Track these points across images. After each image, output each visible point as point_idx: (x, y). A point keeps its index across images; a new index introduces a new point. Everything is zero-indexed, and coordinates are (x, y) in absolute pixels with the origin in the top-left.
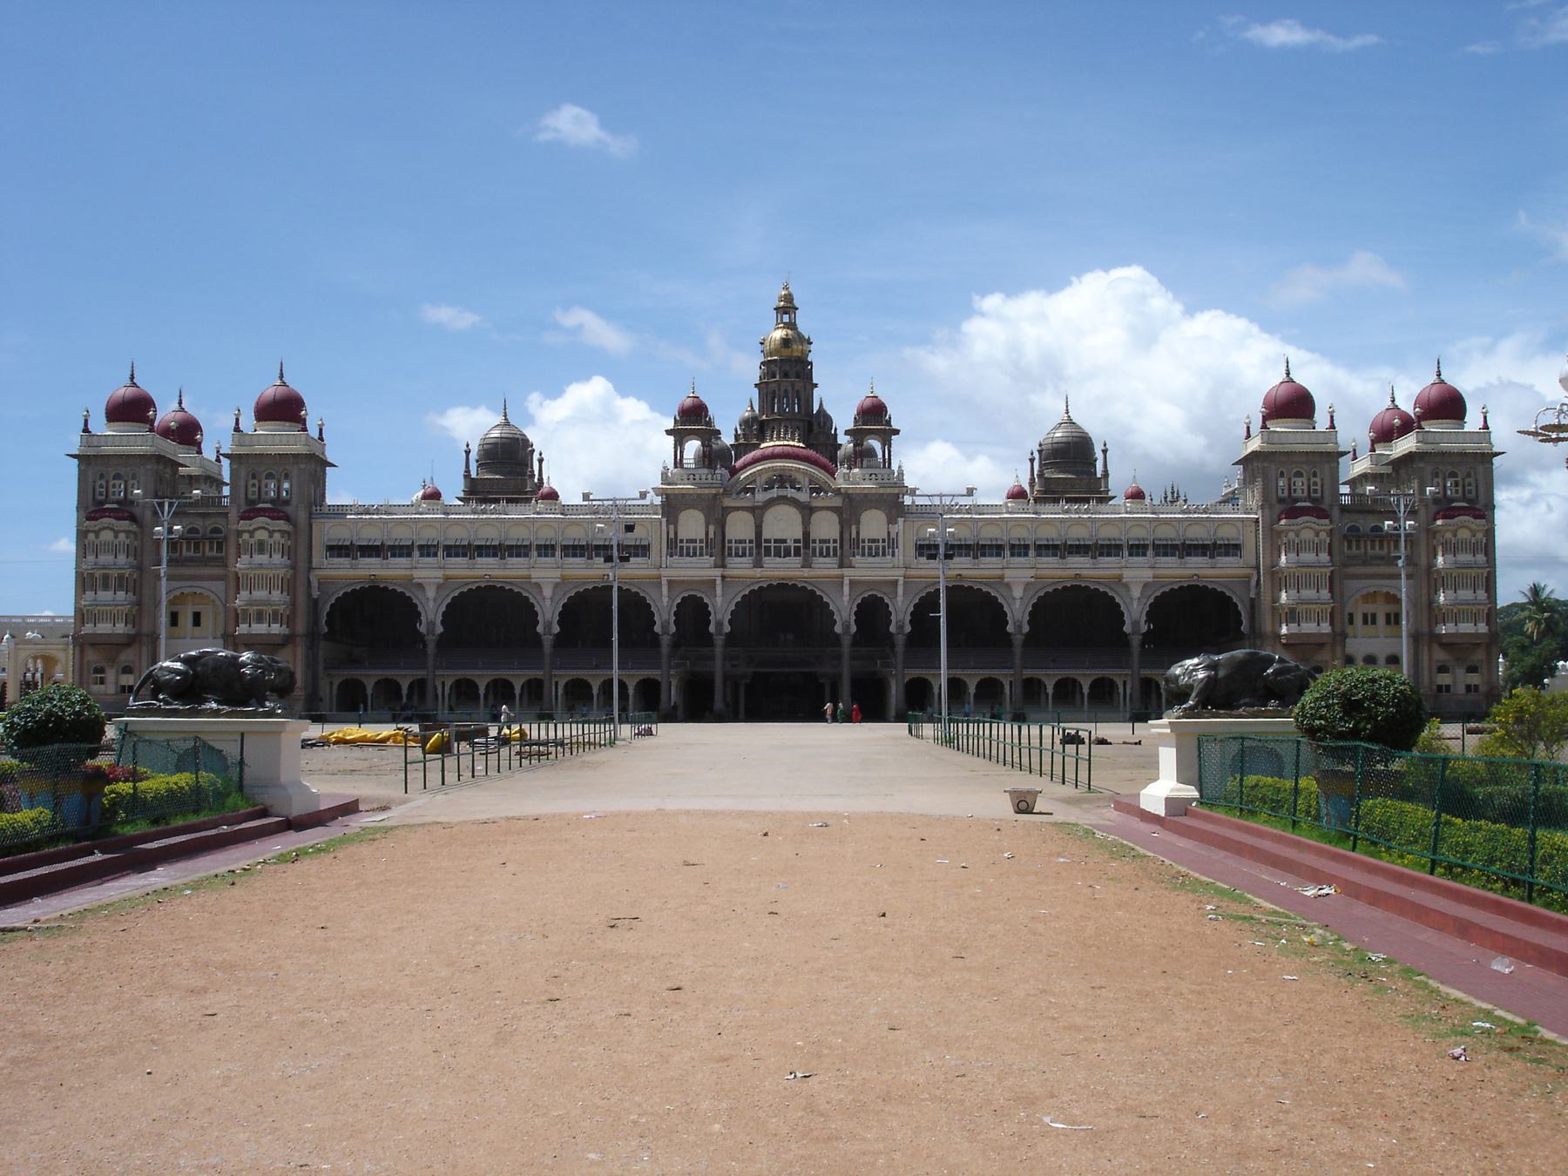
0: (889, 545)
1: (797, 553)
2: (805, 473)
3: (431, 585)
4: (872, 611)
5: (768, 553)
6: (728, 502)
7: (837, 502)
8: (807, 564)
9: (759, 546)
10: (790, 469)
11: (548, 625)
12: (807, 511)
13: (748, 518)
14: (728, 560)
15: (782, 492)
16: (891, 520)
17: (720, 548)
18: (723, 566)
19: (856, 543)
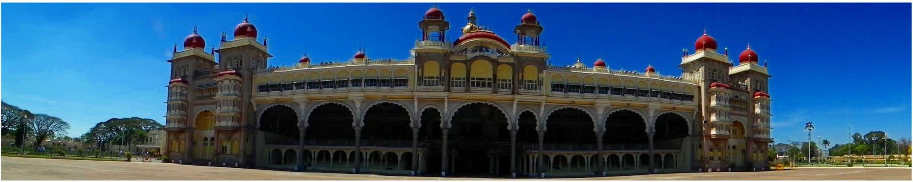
0: (536, 85)
1: (489, 85)
2: (495, 45)
3: (302, 103)
4: (527, 118)
5: (473, 85)
6: (453, 58)
7: (512, 60)
8: (495, 92)
9: (468, 80)
10: (486, 43)
11: (358, 123)
12: (496, 63)
13: (463, 66)
14: (452, 88)
15: (482, 54)
16: (540, 71)
17: (447, 82)
18: (449, 91)
19: (522, 82)
